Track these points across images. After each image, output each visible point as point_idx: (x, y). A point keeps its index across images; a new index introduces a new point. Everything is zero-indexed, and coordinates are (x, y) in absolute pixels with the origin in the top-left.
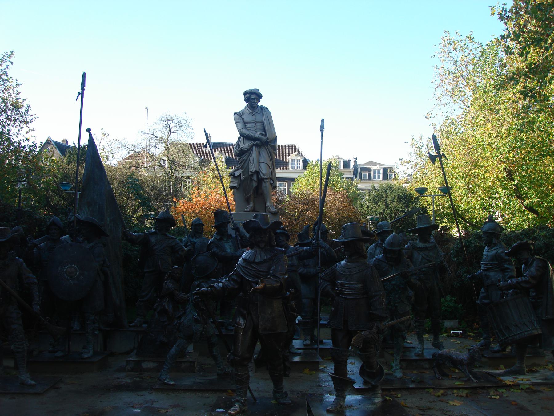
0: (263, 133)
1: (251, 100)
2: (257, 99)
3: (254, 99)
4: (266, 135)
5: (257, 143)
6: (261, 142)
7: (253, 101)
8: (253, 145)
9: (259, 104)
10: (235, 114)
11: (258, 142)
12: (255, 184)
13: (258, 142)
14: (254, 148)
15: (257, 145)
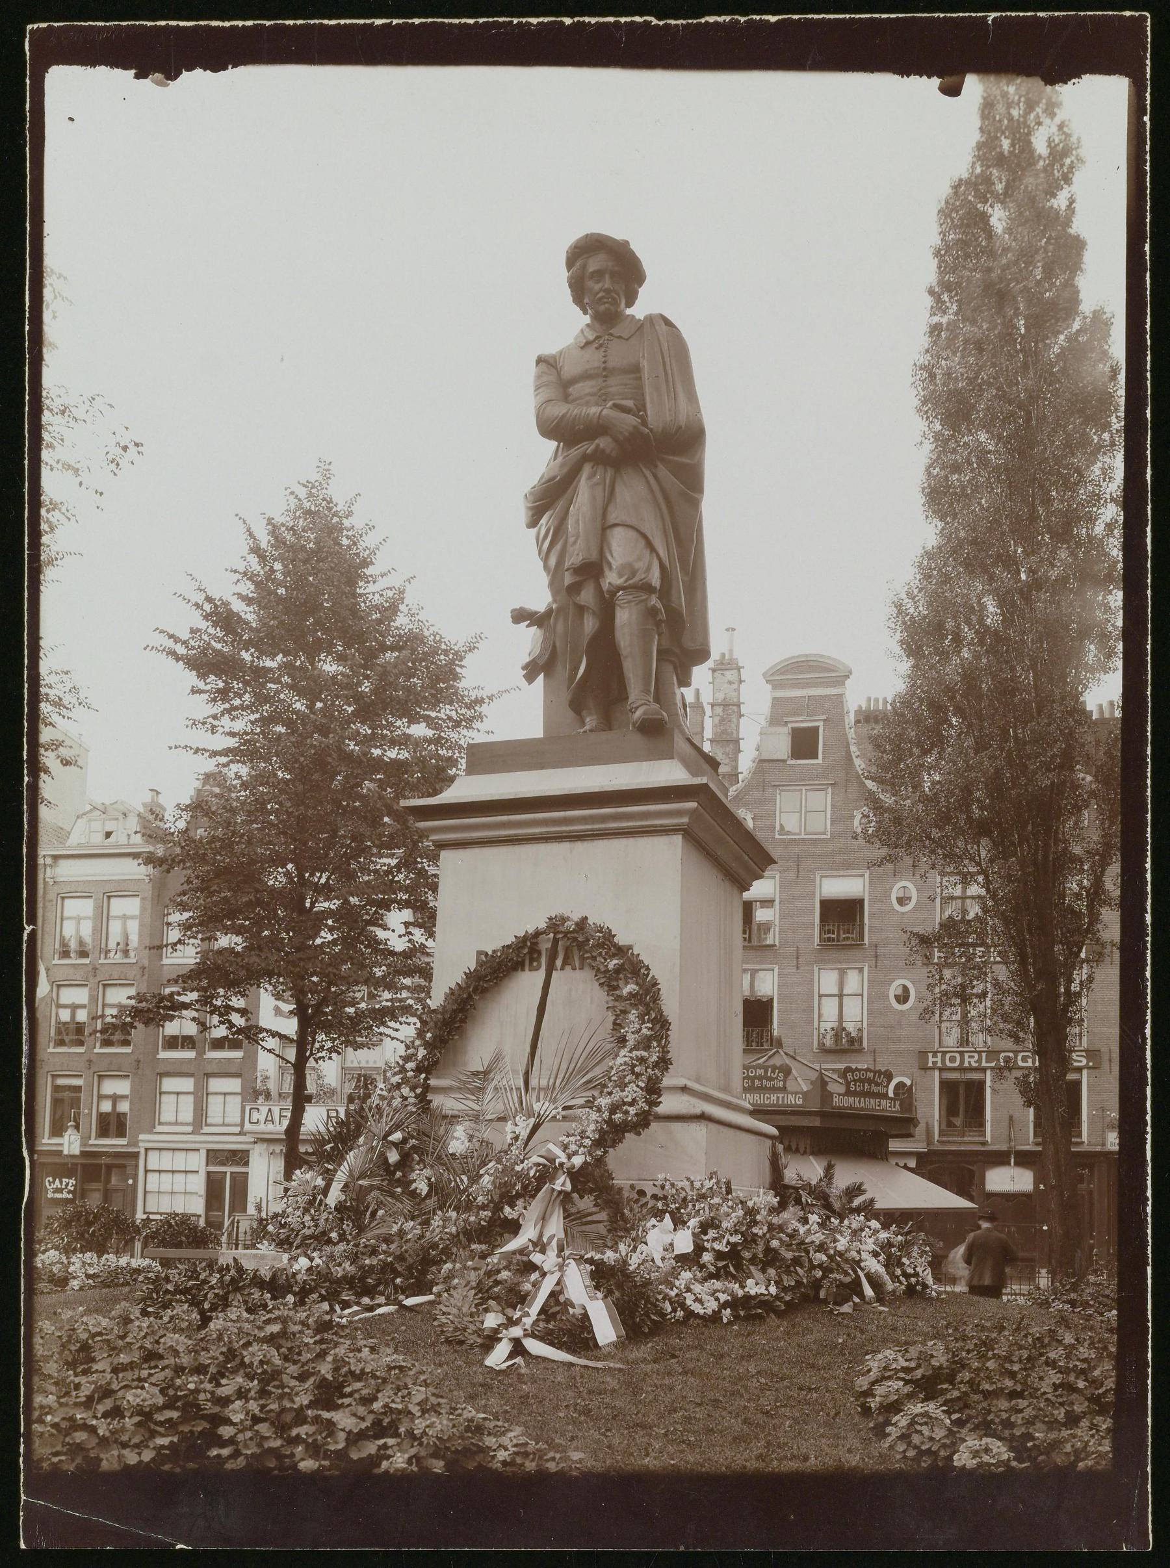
0: (630, 403)
1: (590, 284)
2: (613, 275)
3: (599, 275)
4: (639, 410)
5: (598, 445)
6: (615, 440)
7: (597, 287)
8: (585, 458)
9: (639, 310)
10: (540, 360)
11: (604, 442)
12: (590, 625)
13: (604, 442)
14: (587, 469)
15: (598, 459)
